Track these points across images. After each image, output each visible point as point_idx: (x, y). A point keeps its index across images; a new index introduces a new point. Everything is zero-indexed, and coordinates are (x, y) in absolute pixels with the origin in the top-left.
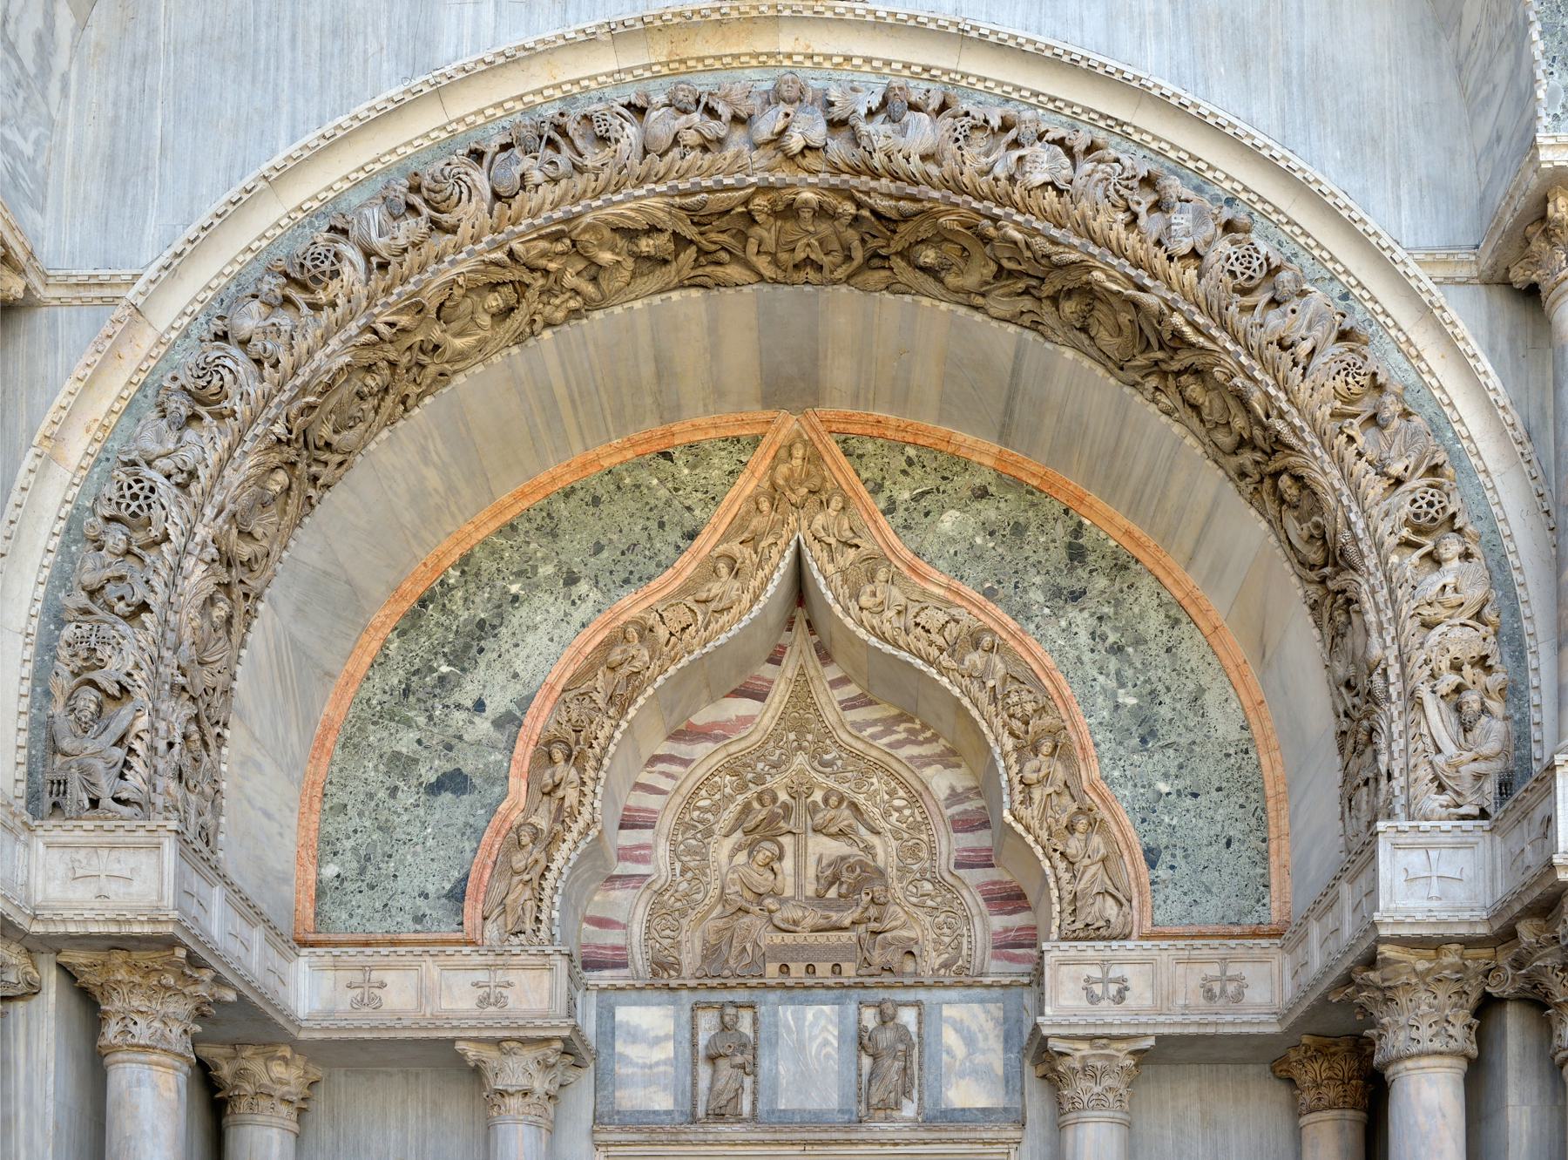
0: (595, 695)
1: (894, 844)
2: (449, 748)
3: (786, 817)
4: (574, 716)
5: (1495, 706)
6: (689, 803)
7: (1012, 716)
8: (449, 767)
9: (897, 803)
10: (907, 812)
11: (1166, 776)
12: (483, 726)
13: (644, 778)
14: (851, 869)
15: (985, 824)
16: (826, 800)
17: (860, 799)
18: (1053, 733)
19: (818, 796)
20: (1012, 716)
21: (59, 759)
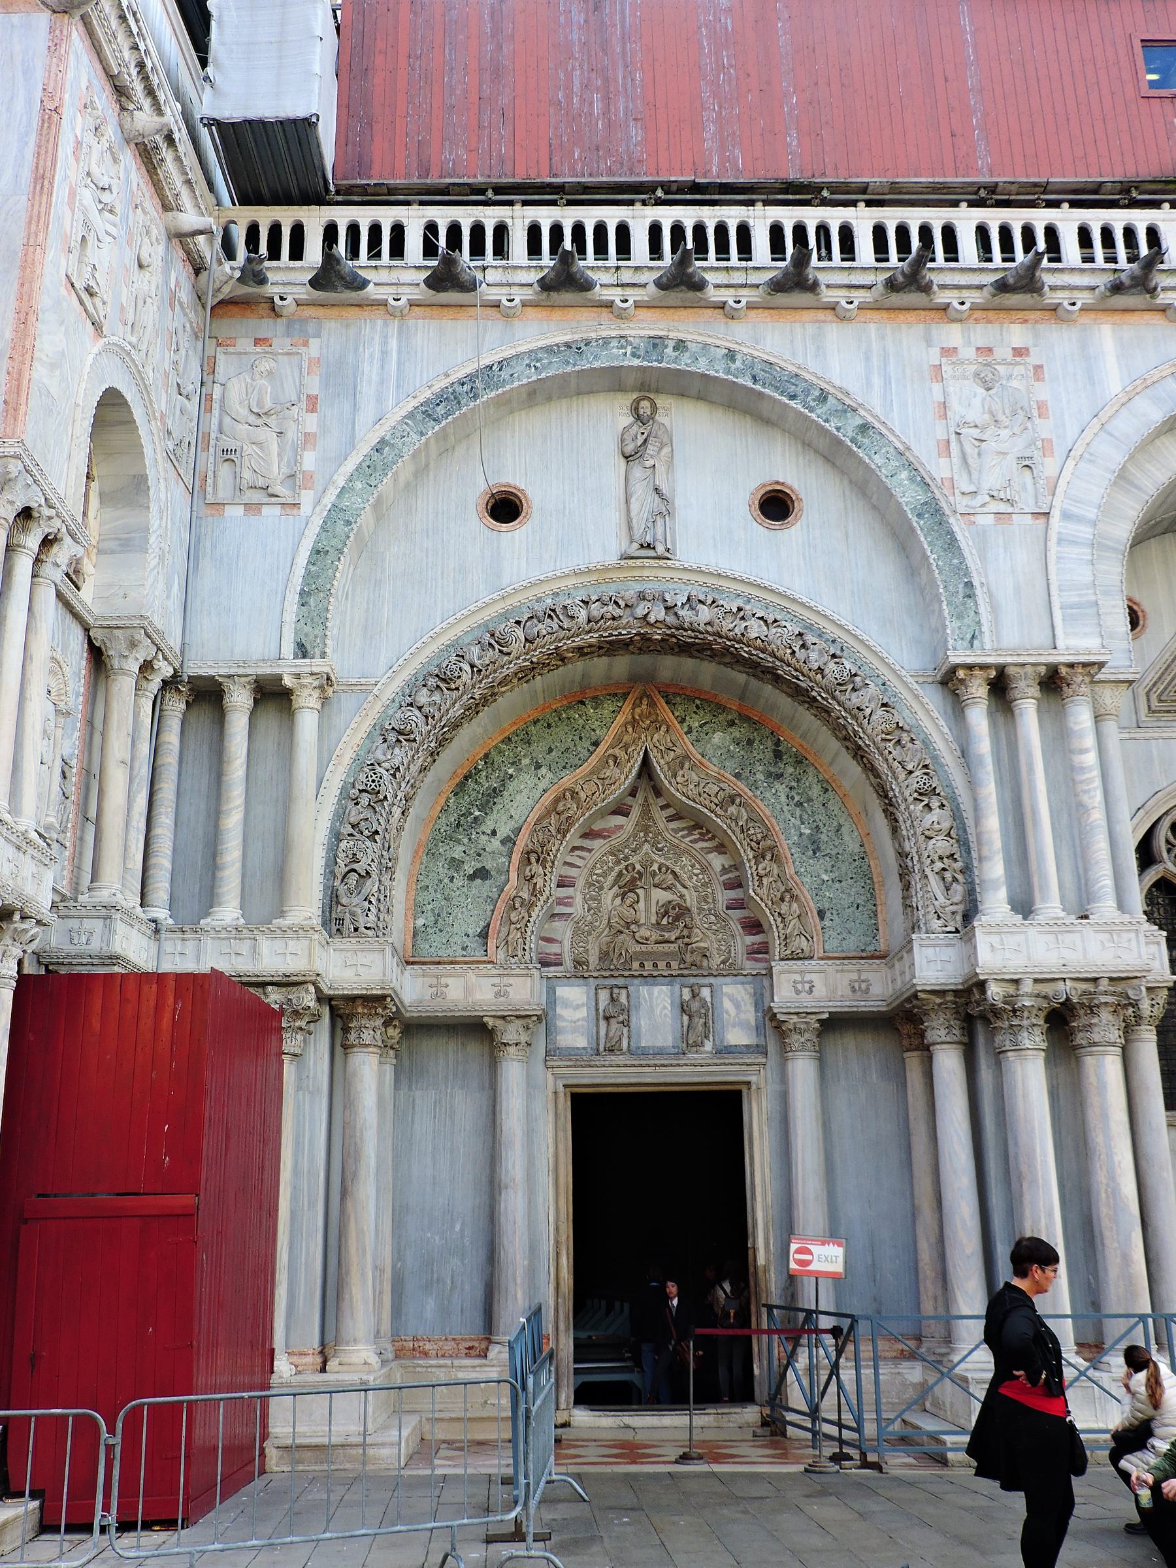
0: (552, 829)
2: (479, 855)
3: (640, 879)
5: (959, 877)
8: (479, 866)
9: (695, 871)
12: (496, 843)
13: (569, 859)
14: (674, 908)
15: (740, 886)
16: (660, 869)
17: (677, 869)
18: (771, 848)
19: (655, 867)
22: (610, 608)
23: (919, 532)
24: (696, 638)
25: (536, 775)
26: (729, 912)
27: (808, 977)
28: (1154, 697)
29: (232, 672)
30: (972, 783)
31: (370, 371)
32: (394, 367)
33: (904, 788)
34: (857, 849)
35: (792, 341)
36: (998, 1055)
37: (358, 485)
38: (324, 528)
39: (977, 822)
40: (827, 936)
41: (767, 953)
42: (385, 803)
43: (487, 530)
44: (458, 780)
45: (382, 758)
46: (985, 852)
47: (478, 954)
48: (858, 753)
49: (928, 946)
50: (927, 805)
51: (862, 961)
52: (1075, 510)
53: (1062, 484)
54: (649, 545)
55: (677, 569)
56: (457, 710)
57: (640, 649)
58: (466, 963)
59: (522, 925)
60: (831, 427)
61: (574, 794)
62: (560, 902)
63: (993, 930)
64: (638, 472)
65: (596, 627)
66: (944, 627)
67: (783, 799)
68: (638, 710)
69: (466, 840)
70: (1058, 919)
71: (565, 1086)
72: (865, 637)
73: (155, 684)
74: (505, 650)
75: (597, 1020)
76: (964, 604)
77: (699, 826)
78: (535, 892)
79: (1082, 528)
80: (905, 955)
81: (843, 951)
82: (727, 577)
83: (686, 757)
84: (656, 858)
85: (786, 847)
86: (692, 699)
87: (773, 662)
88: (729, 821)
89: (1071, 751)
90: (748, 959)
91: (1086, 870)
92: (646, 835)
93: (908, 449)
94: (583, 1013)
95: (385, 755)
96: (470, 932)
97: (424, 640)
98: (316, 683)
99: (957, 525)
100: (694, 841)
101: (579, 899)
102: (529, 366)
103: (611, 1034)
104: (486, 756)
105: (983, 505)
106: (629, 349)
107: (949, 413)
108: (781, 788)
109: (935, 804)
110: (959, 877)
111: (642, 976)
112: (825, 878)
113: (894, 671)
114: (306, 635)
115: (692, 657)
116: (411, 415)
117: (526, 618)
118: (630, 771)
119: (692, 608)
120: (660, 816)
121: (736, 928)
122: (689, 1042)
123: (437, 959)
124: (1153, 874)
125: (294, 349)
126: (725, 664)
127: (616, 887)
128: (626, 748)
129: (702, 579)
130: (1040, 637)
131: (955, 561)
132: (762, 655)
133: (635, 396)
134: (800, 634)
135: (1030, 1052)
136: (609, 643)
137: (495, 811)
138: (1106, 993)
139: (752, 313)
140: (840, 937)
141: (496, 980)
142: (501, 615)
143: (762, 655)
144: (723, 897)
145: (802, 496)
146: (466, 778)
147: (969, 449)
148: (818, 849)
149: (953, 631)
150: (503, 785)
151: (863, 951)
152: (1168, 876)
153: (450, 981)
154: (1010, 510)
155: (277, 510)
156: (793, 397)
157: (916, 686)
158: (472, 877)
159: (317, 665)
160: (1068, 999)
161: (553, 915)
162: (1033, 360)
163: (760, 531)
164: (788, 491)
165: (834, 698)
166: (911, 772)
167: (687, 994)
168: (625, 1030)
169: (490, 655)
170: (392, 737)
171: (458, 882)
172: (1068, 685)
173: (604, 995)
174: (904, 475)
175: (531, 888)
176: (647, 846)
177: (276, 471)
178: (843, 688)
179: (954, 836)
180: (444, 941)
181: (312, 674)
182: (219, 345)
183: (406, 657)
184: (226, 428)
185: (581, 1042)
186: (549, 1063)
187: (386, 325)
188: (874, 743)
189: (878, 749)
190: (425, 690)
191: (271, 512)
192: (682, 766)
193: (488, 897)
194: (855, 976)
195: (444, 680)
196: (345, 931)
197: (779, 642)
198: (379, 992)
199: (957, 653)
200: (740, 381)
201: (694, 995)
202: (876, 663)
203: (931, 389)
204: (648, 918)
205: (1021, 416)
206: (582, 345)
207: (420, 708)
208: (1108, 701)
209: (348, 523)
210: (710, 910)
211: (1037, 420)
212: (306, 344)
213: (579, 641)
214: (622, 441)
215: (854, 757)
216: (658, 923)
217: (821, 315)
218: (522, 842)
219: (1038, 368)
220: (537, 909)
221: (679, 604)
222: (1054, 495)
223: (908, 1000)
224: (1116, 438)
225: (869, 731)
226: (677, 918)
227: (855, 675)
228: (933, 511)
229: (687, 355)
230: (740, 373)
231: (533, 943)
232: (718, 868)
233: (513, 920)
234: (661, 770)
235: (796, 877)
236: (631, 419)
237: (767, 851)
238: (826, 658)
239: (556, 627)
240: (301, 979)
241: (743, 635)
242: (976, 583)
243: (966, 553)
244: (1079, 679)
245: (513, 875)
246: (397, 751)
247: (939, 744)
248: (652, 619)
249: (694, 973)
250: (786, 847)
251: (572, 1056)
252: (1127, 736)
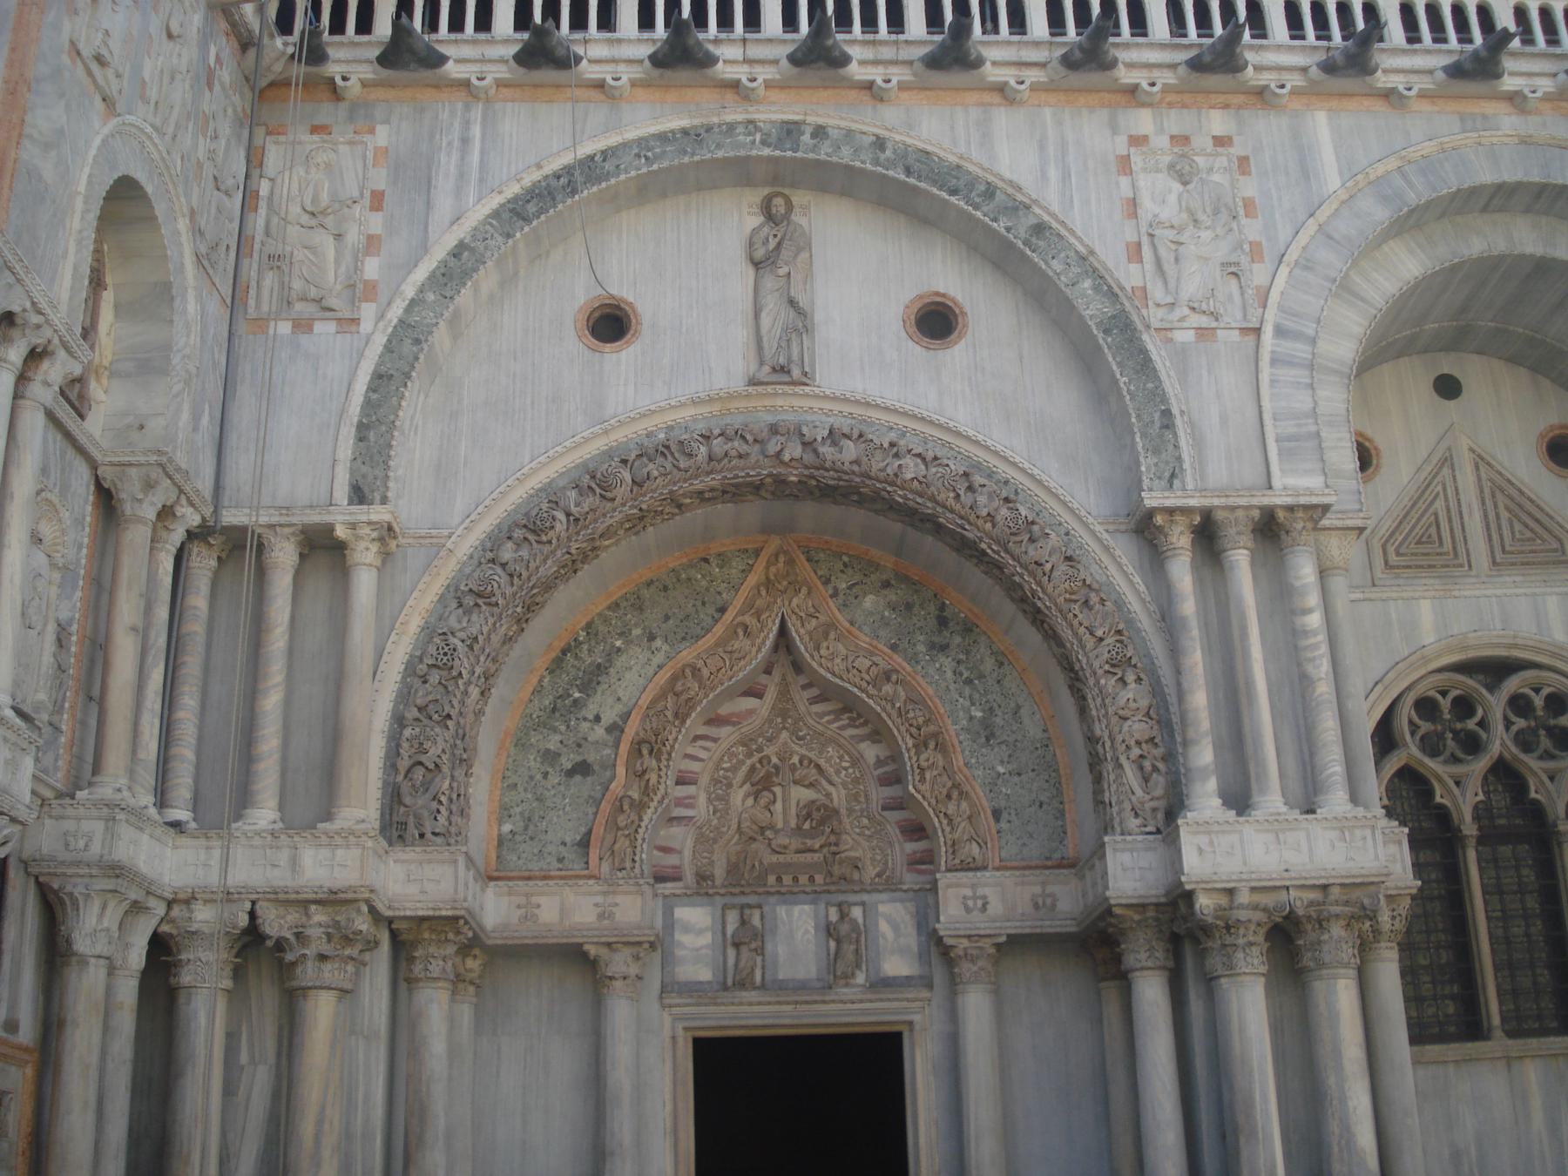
1: (843, 792)
2: (579, 746)
3: (777, 774)
4: (654, 725)
5: (1161, 766)
6: (718, 767)
7: (911, 725)
8: (579, 759)
9: (845, 764)
10: (851, 771)
11: (1002, 762)
12: (599, 732)
13: (690, 750)
16: (801, 762)
17: (822, 762)
18: (935, 735)
19: (795, 759)
20: (911, 725)
21: (402, 809)
22: (736, 444)
23: (1106, 351)
24: (840, 479)
25: (649, 648)
26: (886, 813)
27: (980, 892)
28: (1391, 550)
29: (275, 520)
30: (1175, 652)
31: (448, 163)
32: (475, 157)
33: (1093, 659)
34: (1040, 735)
35: (952, 128)
36: (1209, 981)
37: (431, 297)
38: (389, 348)
39: (1181, 696)
40: (1003, 841)
41: (931, 862)
42: (460, 682)
43: (587, 351)
44: (554, 655)
45: (456, 626)
46: (1191, 734)
47: (577, 867)
48: (1038, 618)
49: (1123, 850)
50: (1122, 680)
51: (1047, 872)
52: (1289, 324)
53: (1274, 296)
54: (782, 368)
55: (816, 396)
56: (550, 568)
57: (773, 493)
58: (562, 878)
59: (632, 830)
60: (1000, 226)
61: (696, 671)
62: (680, 802)
63: (1202, 829)
64: (769, 282)
65: (719, 467)
66: (1138, 464)
67: (949, 674)
68: (773, 569)
69: (563, 728)
70: (1279, 814)
71: (686, 1029)
72: (1044, 477)
73: (178, 536)
74: (608, 495)
75: (725, 948)
76: (1161, 436)
77: (850, 708)
78: (647, 791)
79: (1299, 346)
80: (1097, 863)
81: (1022, 859)
82: (877, 406)
83: (830, 626)
84: (797, 748)
85: (953, 733)
86: (839, 555)
87: (934, 509)
88: (883, 703)
89: (1293, 612)
90: (908, 870)
91: (1312, 755)
92: (784, 720)
93: (1092, 252)
94: (706, 939)
95: (460, 622)
96: (568, 840)
97: (509, 482)
98: (375, 535)
99: (1150, 341)
100: (841, 728)
101: (702, 799)
102: (638, 156)
103: (742, 964)
104: (589, 626)
105: (1182, 319)
106: (758, 137)
107: (1139, 211)
108: (947, 663)
109: (1130, 678)
110: (1161, 766)
111: (778, 892)
112: (1001, 770)
113: (1079, 518)
114: (364, 476)
115: (835, 503)
116: (496, 214)
117: (633, 456)
118: (764, 642)
119: (834, 444)
120: (801, 698)
121: (893, 831)
122: (836, 971)
123: (527, 874)
124: (1394, 763)
125: (358, 138)
126: (876, 512)
127: (747, 786)
128: (758, 615)
129: (847, 409)
130: (1250, 473)
131: (1150, 385)
132: (919, 500)
133: (766, 191)
134: (966, 474)
135: (1248, 978)
136: (736, 486)
137: (599, 693)
138: (1337, 903)
139: (905, 95)
140: (1020, 842)
141: (599, 899)
142: (604, 453)
143: (919, 500)
144: (879, 794)
145: (967, 309)
146: (564, 652)
147: (1163, 252)
148: (993, 735)
149: (1148, 469)
150: (610, 661)
151: (1047, 859)
153: (543, 900)
154: (1214, 324)
155: (331, 327)
156: (953, 192)
157: (1105, 536)
158: (570, 773)
159: (378, 513)
160: (1291, 912)
161: (671, 819)
162: (1237, 150)
163: (916, 351)
164: (950, 304)
165: (1007, 551)
166: (1101, 639)
167: (834, 915)
168: (759, 959)
169: (589, 502)
170: (469, 601)
171: (554, 779)
172: (1287, 532)
173: (733, 919)
174: (1087, 284)
175: (643, 784)
176: (784, 735)
177: (332, 277)
178: (1018, 539)
179: (1154, 716)
180: (536, 851)
181: (370, 523)
182: (269, 133)
183: (487, 502)
184: (273, 230)
185: (705, 974)
186: (667, 1001)
187: (467, 108)
188: (1056, 605)
189: (1061, 611)
190: (510, 545)
191: (324, 328)
192: (826, 639)
193: (590, 797)
194: (1038, 889)
195: (534, 532)
196: (408, 837)
197: (939, 484)
198: (450, 913)
199: (1154, 494)
200: (891, 173)
201: (843, 916)
202: (1058, 509)
203: (1117, 183)
204: (786, 822)
205: (1224, 216)
206: (702, 131)
207: (503, 565)
208: (1335, 552)
209: (417, 342)
210: (862, 811)
211: (1244, 221)
212: (372, 131)
213: (698, 485)
214: (751, 244)
215: (1034, 622)
216: (799, 828)
217: (987, 97)
218: (632, 729)
219: (1243, 161)
220: (649, 811)
221: (819, 439)
222: (1265, 307)
223: (1101, 917)
224: (1338, 243)
225: (1050, 590)
226: (822, 822)
227: (1033, 523)
228: (1123, 327)
229: (827, 143)
230: (890, 164)
231: (645, 854)
232: (871, 760)
233: (622, 823)
234: (801, 640)
235: (965, 770)
236: (762, 219)
237: (932, 740)
238: (996, 503)
239: (669, 466)
240: (350, 896)
241: (896, 475)
242: (1175, 411)
243: (1163, 375)
244: (1299, 525)
245: (621, 770)
246: (474, 617)
247: (1135, 605)
248: (786, 457)
249: (843, 888)
250: (953, 733)
251: (693, 990)
252: (1359, 596)
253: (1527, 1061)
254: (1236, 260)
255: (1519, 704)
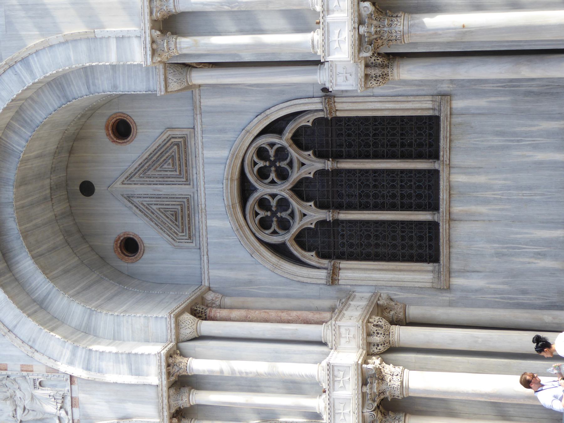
152: (294, 237)
208: (188, 331)
211: (9, 373)
253: (452, 210)
254: (32, 381)
255: (262, 174)
